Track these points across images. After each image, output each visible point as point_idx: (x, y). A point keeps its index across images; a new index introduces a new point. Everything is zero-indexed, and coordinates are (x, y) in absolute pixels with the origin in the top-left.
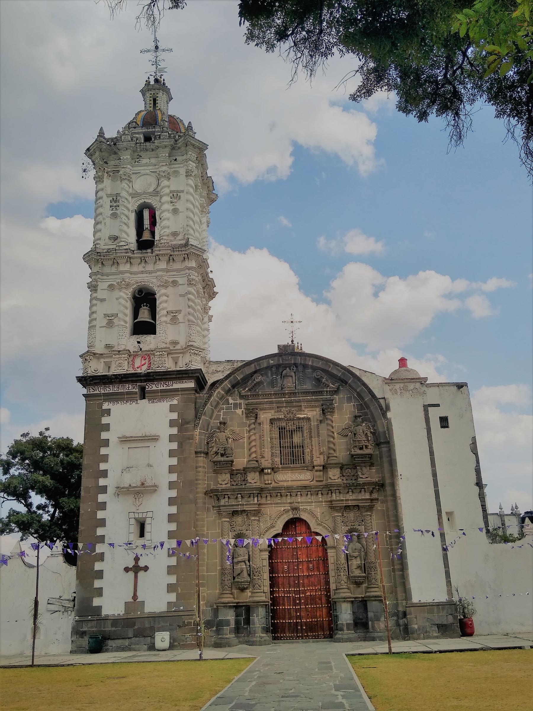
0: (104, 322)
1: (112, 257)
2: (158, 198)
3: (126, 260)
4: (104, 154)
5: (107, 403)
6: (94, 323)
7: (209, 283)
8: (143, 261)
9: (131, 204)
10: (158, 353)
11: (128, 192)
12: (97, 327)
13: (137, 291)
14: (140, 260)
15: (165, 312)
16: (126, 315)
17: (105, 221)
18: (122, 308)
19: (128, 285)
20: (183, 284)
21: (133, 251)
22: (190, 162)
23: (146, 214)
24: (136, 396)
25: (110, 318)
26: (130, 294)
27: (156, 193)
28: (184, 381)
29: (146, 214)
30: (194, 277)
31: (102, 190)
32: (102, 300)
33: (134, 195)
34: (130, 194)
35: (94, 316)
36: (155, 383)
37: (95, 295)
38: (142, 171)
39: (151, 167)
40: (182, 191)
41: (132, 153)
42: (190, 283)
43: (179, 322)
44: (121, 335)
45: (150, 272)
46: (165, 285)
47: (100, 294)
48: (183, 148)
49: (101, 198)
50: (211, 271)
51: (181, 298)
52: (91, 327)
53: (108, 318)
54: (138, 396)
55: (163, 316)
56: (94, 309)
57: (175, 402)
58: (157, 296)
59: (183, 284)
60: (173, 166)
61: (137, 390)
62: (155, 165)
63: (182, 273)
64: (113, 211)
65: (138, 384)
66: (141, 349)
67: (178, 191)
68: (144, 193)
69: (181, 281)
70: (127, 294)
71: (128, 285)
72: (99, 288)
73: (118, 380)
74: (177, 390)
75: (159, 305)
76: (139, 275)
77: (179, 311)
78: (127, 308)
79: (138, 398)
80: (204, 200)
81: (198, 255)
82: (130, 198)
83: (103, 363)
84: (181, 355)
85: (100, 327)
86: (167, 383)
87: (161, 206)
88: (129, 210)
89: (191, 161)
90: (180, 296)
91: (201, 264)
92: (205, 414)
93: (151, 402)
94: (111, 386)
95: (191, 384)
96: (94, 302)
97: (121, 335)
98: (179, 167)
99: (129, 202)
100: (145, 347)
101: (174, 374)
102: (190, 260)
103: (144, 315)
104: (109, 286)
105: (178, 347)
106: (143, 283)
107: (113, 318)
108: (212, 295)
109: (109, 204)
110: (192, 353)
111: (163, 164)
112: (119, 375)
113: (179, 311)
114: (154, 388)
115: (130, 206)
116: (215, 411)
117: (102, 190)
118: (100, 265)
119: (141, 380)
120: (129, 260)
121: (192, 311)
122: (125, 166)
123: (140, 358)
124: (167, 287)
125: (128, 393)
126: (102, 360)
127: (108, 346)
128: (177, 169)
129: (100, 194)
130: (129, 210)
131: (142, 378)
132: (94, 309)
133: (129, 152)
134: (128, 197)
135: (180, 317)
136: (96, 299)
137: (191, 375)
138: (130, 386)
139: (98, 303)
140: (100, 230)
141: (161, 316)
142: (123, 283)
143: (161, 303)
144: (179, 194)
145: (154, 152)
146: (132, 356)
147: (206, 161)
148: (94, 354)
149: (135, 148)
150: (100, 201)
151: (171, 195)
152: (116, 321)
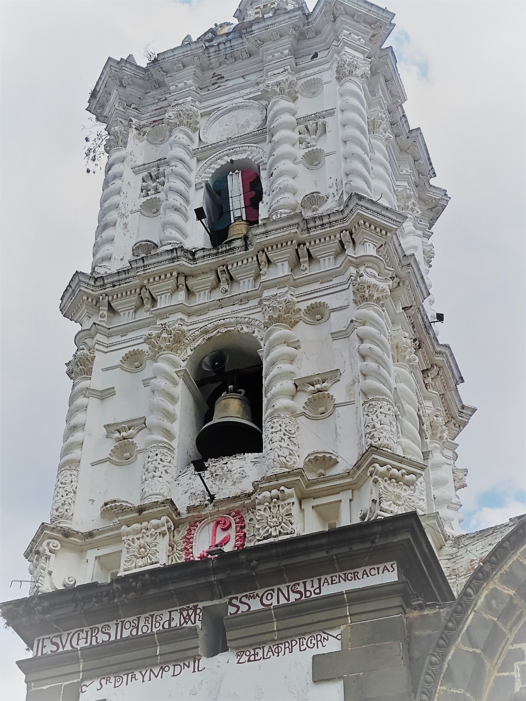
0: (108, 447)
1: (136, 282)
2: (266, 147)
3: (173, 281)
4: (128, 89)
5: (96, 684)
6: (75, 454)
7: (438, 359)
8: (224, 277)
9: (195, 172)
10: (267, 494)
11: (185, 147)
12: (85, 465)
13: (207, 360)
14: (213, 277)
15: (288, 385)
16: (170, 417)
17: (125, 220)
18: (159, 400)
19: (178, 340)
20: (341, 308)
21: (193, 254)
22: (347, 49)
23: (235, 185)
24: (192, 643)
25: (124, 434)
26: (184, 364)
27: (263, 133)
28: (360, 571)
29: (235, 185)
30: (373, 281)
31: (123, 160)
32: (104, 395)
33: (202, 154)
34: (194, 153)
35: (78, 436)
36: (260, 592)
37: (84, 384)
38: (225, 105)
39: (247, 91)
40: (331, 113)
41: (199, 73)
42: (362, 296)
43: (335, 406)
44: (151, 467)
45: (243, 299)
46: (287, 317)
47: (97, 381)
48: (328, 27)
49: (119, 176)
50: (440, 317)
51: (337, 344)
52: (69, 465)
53: (117, 435)
54: (201, 642)
55: (282, 394)
56: (79, 418)
57: (332, 645)
58: (262, 353)
59: (341, 308)
60: (303, 74)
61: (199, 624)
62: (258, 84)
63: (335, 281)
64: (149, 198)
65: (201, 605)
66: (212, 497)
67: (317, 116)
68: (230, 141)
69: (332, 302)
70: (174, 364)
71: (178, 340)
72: (96, 368)
73: (132, 595)
74: (335, 601)
75: (271, 381)
76: (212, 314)
77: (334, 375)
78: (173, 399)
79: (200, 651)
80: (406, 184)
81: (383, 228)
82: (193, 162)
83: (92, 561)
84: (344, 497)
85: (93, 464)
86: (301, 588)
87: (273, 149)
88: (188, 183)
89: (350, 46)
90: (336, 336)
91: (403, 273)
92: (449, 677)
93: (245, 658)
94: (113, 624)
95: (388, 575)
96: (81, 401)
97: (151, 467)
98: (319, 72)
99: (190, 169)
100: (224, 490)
101: (319, 548)
102: (358, 246)
103: (231, 409)
104: (126, 358)
105: (338, 470)
106: (223, 330)
107: (131, 431)
108: (458, 416)
109: (139, 184)
110: (382, 476)
111: (276, 72)
112: (135, 576)
113: (334, 375)
114: (256, 605)
115: (193, 178)
116: (488, 665)
117: (123, 160)
118: (104, 310)
119: (210, 586)
120: (184, 281)
121: (374, 365)
122: (180, 102)
123: (212, 525)
124: (293, 325)
125: (170, 636)
126: (92, 554)
127: (111, 509)
128: (316, 76)
129: (115, 169)
130: (188, 183)
131: (213, 578)
132: (79, 418)
133: (191, 69)
134: (186, 158)
135: (338, 392)
136: (88, 392)
137: (379, 542)
138: (176, 616)
139: (93, 402)
140: (111, 240)
141: (274, 396)
142: (164, 335)
143: (273, 364)
144: (320, 121)
145: (253, 59)
146: (184, 523)
147: (395, 70)
148: (67, 534)
149: (205, 58)
150: (118, 182)
151: (302, 127)
152: (140, 440)
